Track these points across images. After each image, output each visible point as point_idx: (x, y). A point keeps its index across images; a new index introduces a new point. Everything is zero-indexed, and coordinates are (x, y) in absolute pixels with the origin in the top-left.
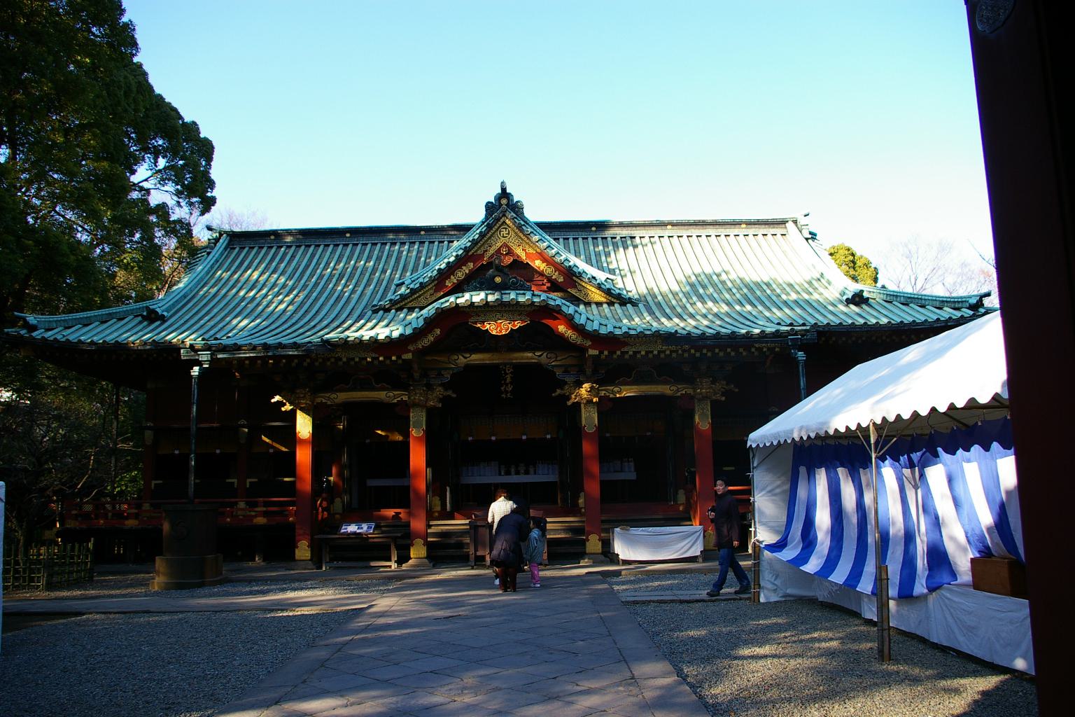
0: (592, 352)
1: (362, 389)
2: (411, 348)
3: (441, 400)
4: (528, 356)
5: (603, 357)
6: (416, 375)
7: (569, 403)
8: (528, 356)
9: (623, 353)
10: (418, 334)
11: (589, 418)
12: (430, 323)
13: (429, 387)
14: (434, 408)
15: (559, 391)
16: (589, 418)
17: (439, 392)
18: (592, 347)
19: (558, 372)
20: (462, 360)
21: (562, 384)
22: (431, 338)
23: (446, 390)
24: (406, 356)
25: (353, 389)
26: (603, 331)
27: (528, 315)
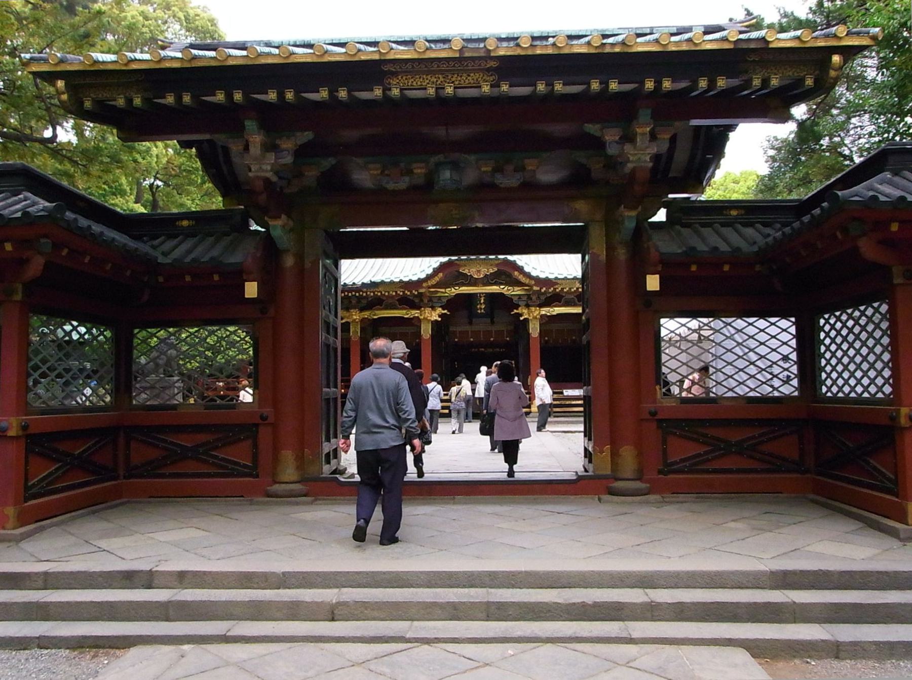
0: (535, 288)
1: (391, 309)
2: (424, 285)
3: (440, 316)
4: (495, 289)
5: (543, 290)
6: (426, 301)
7: (522, 318)
8: (495, 289)
9: (555, 289)
10: (429, 277)
11: (534, 330)
12: (436, 271)
13: (433, 308)
14: (436, 321)
15: (515, 311)
16: (534, 330)
17: (439, 310)
18: (535, 285)
19: (515, 299)
20: (453, 291)
21: (517, 306)
22: (437, 279)
23: (444, 309)
24: (421, 291)
25: (386, 308)
26: (542, 276)
27: (497, 265)
